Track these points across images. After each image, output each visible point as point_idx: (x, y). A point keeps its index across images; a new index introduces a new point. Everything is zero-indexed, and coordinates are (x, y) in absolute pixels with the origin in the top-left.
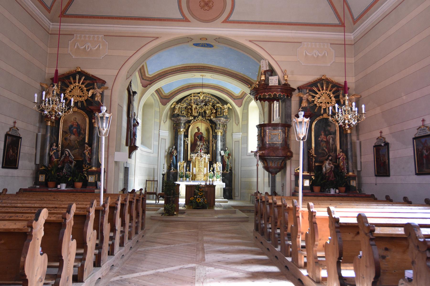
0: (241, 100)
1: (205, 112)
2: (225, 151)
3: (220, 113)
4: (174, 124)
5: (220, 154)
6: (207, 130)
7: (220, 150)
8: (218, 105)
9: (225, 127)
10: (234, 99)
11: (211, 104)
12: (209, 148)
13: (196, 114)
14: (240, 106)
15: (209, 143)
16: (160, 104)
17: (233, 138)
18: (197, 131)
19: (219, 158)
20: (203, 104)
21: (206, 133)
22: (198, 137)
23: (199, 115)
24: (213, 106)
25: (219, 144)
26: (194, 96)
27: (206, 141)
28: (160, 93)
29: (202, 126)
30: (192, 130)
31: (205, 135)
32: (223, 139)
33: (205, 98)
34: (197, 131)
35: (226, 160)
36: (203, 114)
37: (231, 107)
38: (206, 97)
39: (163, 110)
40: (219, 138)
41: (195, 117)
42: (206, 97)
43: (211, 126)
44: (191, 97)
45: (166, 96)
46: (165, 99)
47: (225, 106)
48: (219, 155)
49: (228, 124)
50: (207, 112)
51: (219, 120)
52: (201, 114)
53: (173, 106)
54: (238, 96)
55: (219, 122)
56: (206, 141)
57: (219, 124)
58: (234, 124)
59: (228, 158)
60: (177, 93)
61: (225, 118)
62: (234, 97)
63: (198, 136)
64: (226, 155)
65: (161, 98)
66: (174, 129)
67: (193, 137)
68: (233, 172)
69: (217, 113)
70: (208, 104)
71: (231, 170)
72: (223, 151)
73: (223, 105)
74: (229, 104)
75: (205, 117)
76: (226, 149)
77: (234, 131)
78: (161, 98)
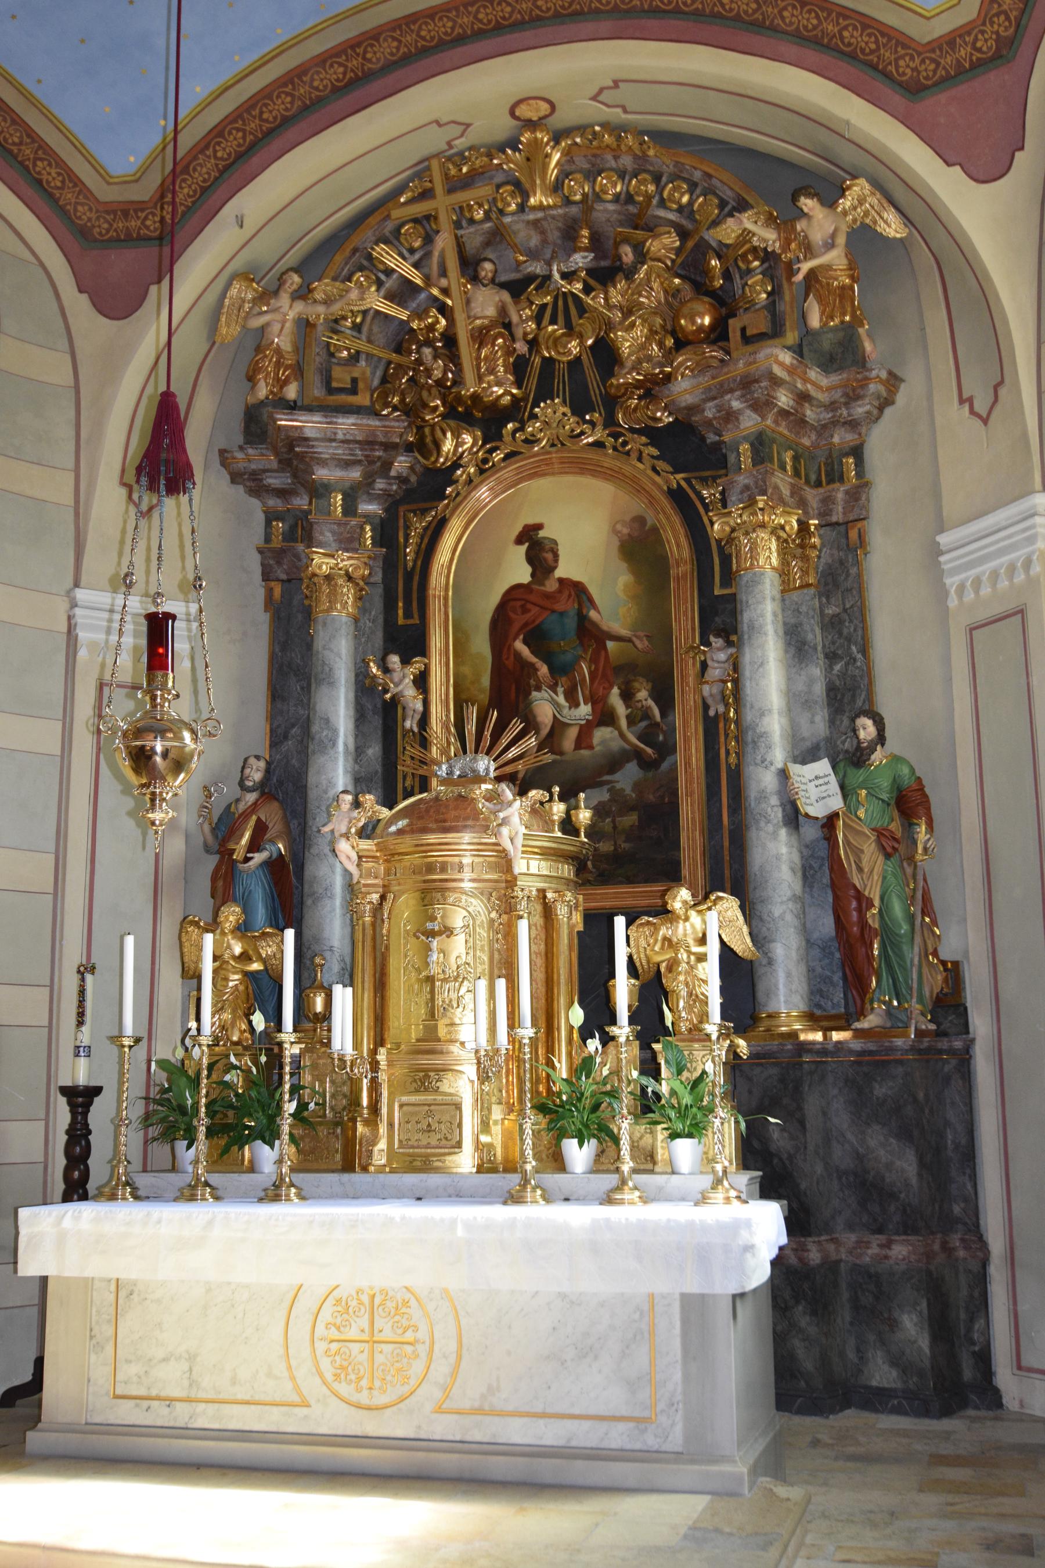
0: (993, 79)
1: (605, 355)
2: (850, 759)
3: (758, 323)
4: (271, 516)
5: (794, 816)
6: (639, 548)
7: (778, 756)
8: (729, 231)
9: (835, 476)
10: (914, 89)
11: (664, 244)
12: (666, 749)
13: (501, 390)
14: (987, 170)
15: (665, 697)
16: (79, 305)
17: (942, 593)
18: (522, 574)
19: (777, 856)
20: (580, 260)
21: (624, 578)
22: (536, 638)
23: (544, 393)
24: (691, 267)
25: (773, 685)
26: (455, 185)
27: (625, 675)
28: (51, 175)
29: (584, 521)
30: (471, 562)
31: (614, 600)
32: (832, 625)
33: (577, 189)
34: (522, 574)
35: (871, 873)
36: (591, 384)
37: (892, 227)
38: (590, 176)
39: (113, 363)
40: (765, 610)
41: (491, 421)
42: (590, 176)
43: (678, 497)
44: (427, 194)
45: (127, 210)
46: (129, 239)
47: (818, 220)
48: (777, 814)
49: (879, 443)
50: (628, 342)
51: (747, 384)
52: (561, 378)
53: (229, 330)
54: (950, 41)
55: (750, 422)
56: (625, 675)
57: (761, 445)
58: (951, 415)
59: (895, 846)
60: (242, 156)
61: (829, 363)
62: (906, 68)
63: (540, 625)
64: (868, 812)
65: (84, 233)
66: (267, 576)
67: (481, 645)
68: (980, 1024)
69: (723, 301)
70: (627, 254)
71: (950, 1006)
72: (823, 766)
73: (786, 219)
74: (860, 188)
75: (611, 403)
76: (867, 729)
77: (951, 507)
78: (84, 233)
